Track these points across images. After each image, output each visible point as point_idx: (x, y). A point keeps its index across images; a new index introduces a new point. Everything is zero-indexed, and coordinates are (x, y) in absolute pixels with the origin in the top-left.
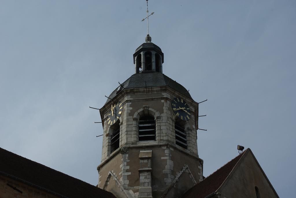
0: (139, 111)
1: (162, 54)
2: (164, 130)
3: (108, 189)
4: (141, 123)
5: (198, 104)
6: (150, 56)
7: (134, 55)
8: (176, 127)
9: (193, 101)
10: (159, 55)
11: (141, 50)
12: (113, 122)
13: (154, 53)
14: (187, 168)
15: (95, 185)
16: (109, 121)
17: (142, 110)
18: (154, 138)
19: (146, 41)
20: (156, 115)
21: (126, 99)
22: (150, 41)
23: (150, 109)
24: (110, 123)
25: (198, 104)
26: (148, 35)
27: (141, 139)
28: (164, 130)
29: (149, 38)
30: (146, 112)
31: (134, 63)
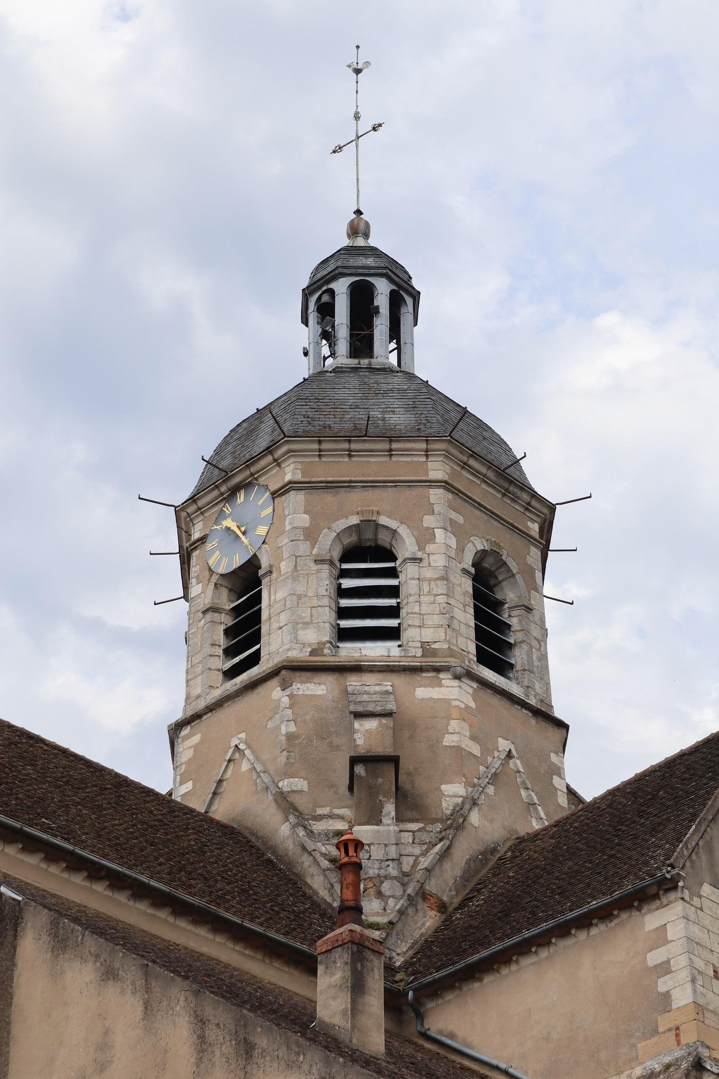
0: (342, 524)
1: (416, 296)
3: (221, 812)
4: (344, 574)
5: (552, 508)
6: (362, 297)
7: (307, 293)
9: (534, 495)
10: (404, 294)
13: (383, 289)
14: (509, 755)
15: (163, 790)
16: (212, 552)
17: (354, 520)
18: (393, 634)
19: (349, 236)
20: (407, 546)
21: (290, 472)
22: (366, 235)
23: (383, 520)
24: (219, 563)
25: (552, 508)
26: (358, 212)
27: (345, 635)
29: (358, 228)
30: (368, 535)
31: (305, 321)
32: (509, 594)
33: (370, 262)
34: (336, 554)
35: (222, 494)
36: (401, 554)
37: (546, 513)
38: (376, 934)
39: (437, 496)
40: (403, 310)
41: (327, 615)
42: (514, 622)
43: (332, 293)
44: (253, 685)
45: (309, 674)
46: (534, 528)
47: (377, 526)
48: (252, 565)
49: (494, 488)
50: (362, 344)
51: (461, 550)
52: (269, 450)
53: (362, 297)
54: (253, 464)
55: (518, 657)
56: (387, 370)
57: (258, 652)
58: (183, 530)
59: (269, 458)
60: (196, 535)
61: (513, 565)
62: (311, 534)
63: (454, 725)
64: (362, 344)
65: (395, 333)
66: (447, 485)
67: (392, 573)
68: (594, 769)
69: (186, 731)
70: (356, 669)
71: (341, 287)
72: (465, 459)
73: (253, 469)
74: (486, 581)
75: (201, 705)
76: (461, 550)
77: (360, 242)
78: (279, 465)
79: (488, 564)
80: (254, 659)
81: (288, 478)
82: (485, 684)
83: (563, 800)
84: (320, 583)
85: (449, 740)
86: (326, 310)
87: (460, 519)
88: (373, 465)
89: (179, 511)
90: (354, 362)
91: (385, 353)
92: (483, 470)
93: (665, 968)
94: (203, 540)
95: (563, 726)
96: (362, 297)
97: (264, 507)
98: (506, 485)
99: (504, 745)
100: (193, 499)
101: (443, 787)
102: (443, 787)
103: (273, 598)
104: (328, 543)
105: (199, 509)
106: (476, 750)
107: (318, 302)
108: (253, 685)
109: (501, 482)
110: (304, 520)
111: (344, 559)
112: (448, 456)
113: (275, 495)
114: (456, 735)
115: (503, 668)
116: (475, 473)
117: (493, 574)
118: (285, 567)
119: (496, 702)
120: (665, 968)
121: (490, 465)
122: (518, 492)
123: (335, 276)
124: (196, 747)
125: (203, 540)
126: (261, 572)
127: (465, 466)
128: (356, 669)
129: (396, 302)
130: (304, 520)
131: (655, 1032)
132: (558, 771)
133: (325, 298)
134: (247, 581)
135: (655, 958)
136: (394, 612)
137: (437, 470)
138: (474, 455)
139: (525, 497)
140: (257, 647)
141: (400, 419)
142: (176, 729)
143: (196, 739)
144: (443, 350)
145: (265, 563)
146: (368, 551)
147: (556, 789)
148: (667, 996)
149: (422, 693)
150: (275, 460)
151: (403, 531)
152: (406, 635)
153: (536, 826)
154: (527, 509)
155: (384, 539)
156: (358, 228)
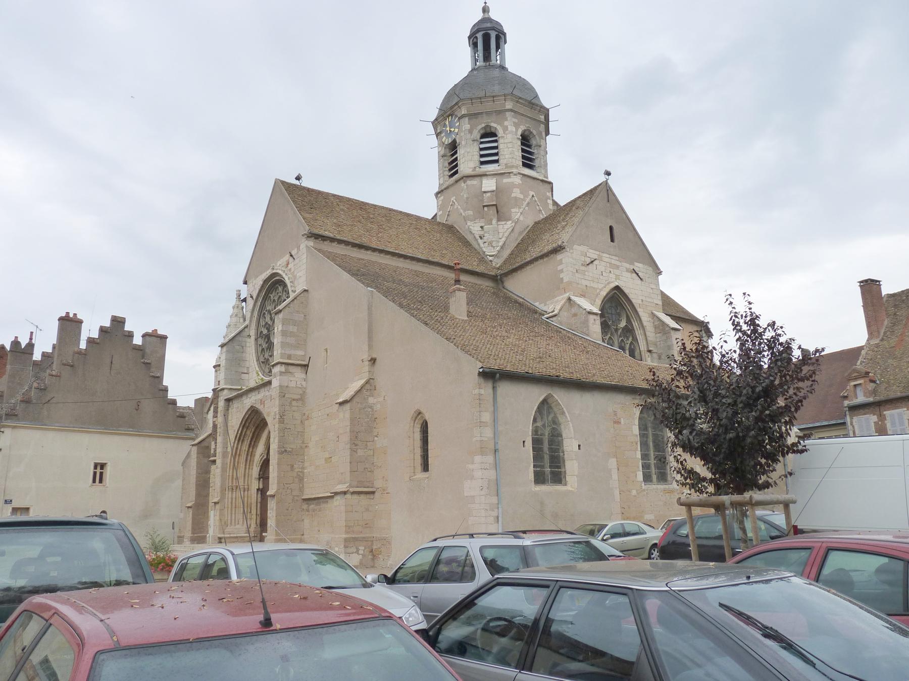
0: (480, 127)
1: (505, 34)
2: (509, 148)
4: (482, 143)
5: (548, 110)
6: (487, 38)
7: (469, 38)
8: (522, 144)
10: (501, 37)
11: (478, 31)
13: (493, 35)
17: (483, 125)
18: (497, 161)
20: (500, 133)
21: (464, 111)
23: (493, 125)
27: (482, 163)
28: (509, 148)
33: (489, 25)
34: (479, 137)
37: (546, 112)
38: (491, 258)
43: (476, 38)
44: (457, 181)
47: (490, 127)
48: (454, 142)
50: (487, 57)
51: (517, 130)
52: (456, 104)
53: (487, 38)
58: (435, 129)
61: (535, 132)
62: (471, 131)
63: (515, 190)
64: (487, 57)
66: (511, 110)
67: (496, 141)
68: (563, 197)
70: (484, 175)
71: (480, 36)
74: (525, 140)
75: (443, 188)
76: (517, 130)
80: (456, 172)
83: (551, 207)
85: (513, 195)
87: (516, 121)
88: (489, 106)
91: (496, 59)
93: (562, 271)
95: (550, 183)
96: (487, 38)
99: (531, 193)
100: (436, 119)
103: (461, 152)
104: (476, 134)
106: (522, 197)
108: (457, 181)
110: (468, 126)
111: (483, 136)
112: (512, 100)
113: (459, 118)
114: (516, 193)
115: (530, 167)
116: (521, 104)
118: (463, 143)
119: (528, 180)
120: (562, 271)
121: (526, 100)
123: (478, 31)
127: (517, 102)
128: (484, 175)
129: (498, 38)
130: (468, 126)
134: (453, 147)
135: (559, 268)
136: (497, 154)
137: (509, 105)
138: (520, 98)
141: (497, 89)
142: (437, 194)
146: (489, 134)
149: (505, 180)
151: (499, 127)
152: (501, 161)
153: (542, 217)
155: (493, 130)
156: (485, 10)
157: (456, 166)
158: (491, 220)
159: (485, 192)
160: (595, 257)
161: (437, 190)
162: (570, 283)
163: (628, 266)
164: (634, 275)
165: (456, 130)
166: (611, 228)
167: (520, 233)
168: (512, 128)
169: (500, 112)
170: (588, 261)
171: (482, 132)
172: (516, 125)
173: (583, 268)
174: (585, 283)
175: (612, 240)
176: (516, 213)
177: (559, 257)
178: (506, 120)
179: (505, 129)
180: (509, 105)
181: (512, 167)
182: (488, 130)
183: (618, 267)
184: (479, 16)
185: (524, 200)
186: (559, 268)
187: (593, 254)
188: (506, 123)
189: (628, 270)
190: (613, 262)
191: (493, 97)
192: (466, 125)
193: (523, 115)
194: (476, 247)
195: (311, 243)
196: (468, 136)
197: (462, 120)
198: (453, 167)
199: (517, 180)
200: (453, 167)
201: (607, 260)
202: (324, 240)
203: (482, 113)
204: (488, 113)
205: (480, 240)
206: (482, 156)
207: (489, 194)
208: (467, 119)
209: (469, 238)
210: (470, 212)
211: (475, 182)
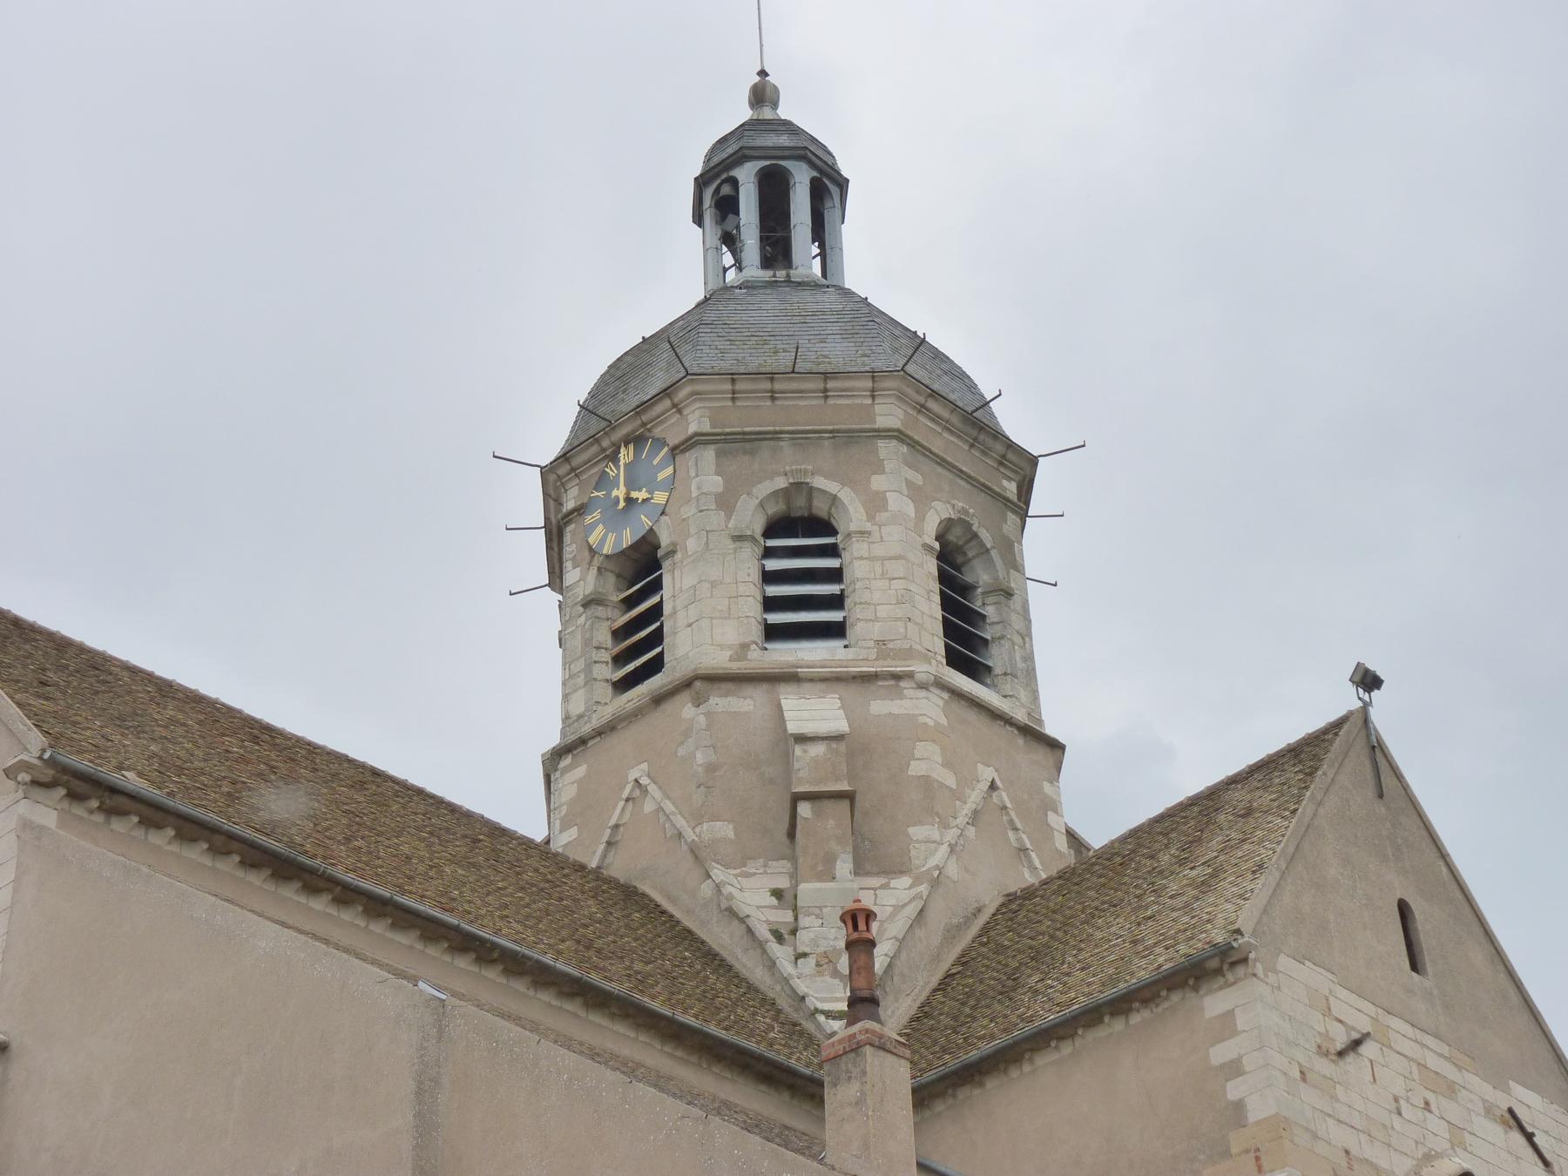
0: (766, 488)
1: (843, 184)
2: (891, 592)
4: (769, 553)
5: (1033, 461)
6: (770, 188)
7: (701, 183)
9: (1011, 445)
10: (829, 186)
12: (618, 540)
13: (801, 179)
14: (993, 786)
16: (593, 526)
17: (781, 483)
18: (835, 631)
20: (852, 516)
21: (696, 421)
22: (775, 105)
23: (819, 482)
24: (603, 540)
25: (1033, 461)
26: (763, 73)
27: (774, 633)
28: (891, 592)
29: (762, 95)
30: (800, 503)
31: (698, 219)
32: (979, 575)
33: (784, 140)
34: (758, 527)
35: (604, 450)
36: (840, 525)
37: (1023, 466)
39: (888, 450)
40: (828, 204)
41: (754, 608)
42: (990, 611)
43: (734, 182)
44: (658, 700)
45: (730, 685)
46: (1011, 488)
47: (811, 491)
49: (959, 437)
50: (777, 250)
52: (666, 392)
53: (774, 189)
54: (645, 411)
55: (996, 658)
56: (813, 286)
57: (661, 655)
58: (552, 495)
59: (667, 403)
60: (570, 504)
61: (985, 535)
62: (725, 502)
63: (922, 749)
64: (777, 250)
65: (819, 231)
66: (899, 436)
67: (832, 551)
68: (1102, 804)
69: (566, 761)
70: (790, 677)
71: (747, 175)
72: (921, 399)
73: (644, 418)
75: (586, 729)
76: (920, 517)
77: (767, 114)
78: (680, 411)
79: (955, 536)
80: (656, 666)
81: (692, 428)
82: (957, 694)
83: (1061, 843)
84: (745, 567)
85: (916, 769)
86: (728, 206)
87: (918, 479)
88: (803, 410)
89: (546, 472)
90: (766, 275)
92: (945, 414)
93: (1234, 1069)
94: (580, 510)
95: (1056, 747)
96: (774, 189)
97: (661, 467)
98: (975, 433)
99: (987, 773)
100: (564, 457)
101: (911, 830)
102: (911, 830)
103: (676, 585)
105: (573, 470)
106: (950, 780)
107: (715, 196)
108: (658, 700)
109: (969, 429)
110: (715, 483)
111: (769, 533)
112: (901, 398)
113: (675, 451)
114: (927, 762)
116: (936, 418)
117: (959, 549)
118: (692, 544)
119: (972, 716)
120: (1234, 1069)
121: (954, 407)
122: (990, 442)
123: (740, 158)
124: (580, 783)
125: (580, 510)
126: (660, 553)
127: (921, 409)
128: (790, 677)
129: (819, 193)
130: (715, 483)
131: (1226, 1154)
132: (1053, 806)
133: (726, 190)
134: (643, 566)
135: (1220, 1054)
136: (836, 602)
137: (889, 414)
138: (934, 394)
139: (999, 448)
140: (659, 650)
141: (838, 352)
143: (581, 771)
144: (882, 254)
145: (665, 540)
146: (801, 526)
147: (1052, 829)
148: (1239, 1106)
149: (880, 706)
150: (674, 405)
151: (846, 495)
153: (1029, 879)
154: (1001, 463)
155: (820, 508)
156: (762, 95)
157: (657, 638)
158: (830, 859)
159: (802, 739)
160: (1364, 1025)
161: (553, 739)
162: (1279, 1126)
163: (1487, 1091)
164: (1518, 1138)
165: (660, 497)
166: (1404, 909)
167: (951, 933)
168: (899, 503)
169: (855, 439)
170: (1341, 1040)
171: (775, 508)
172: (918, 495)
173: (1324, 1067)
174: (1340, 1136)
175: (1415, 966)
176: (929, 844)
177: (1215, 1002)
178: (880, 470)
179: (876, 504)
180: (889, 414)
181: (909, 654)
182: (799, 506)
183: (1451, 1090)
184: (743, 113)
185: (958, 795)
186: (1220, 1054)
187: (1356, 1014)
188: (878, 482)
189: (1489, 1111)
190: (1433, 1062)
191: (826, 376)
192: (705, 474)
193: (942, 462)
194: (755, 972)
195: (46, 813)
196: (716, 519)
197: (689, 458)
198: (638, 647)
199: (930, 708)
200: (638, 647)
201: (1407, 1047)
202: (111, 812)
203: (775, 436)
204: (804, 438)
205: (774, 948)
206: (770, 604)
207: (817, 750)
208: (709, 454)
209: (721, 937)
210: (725, 830)
211: (747, 704)
